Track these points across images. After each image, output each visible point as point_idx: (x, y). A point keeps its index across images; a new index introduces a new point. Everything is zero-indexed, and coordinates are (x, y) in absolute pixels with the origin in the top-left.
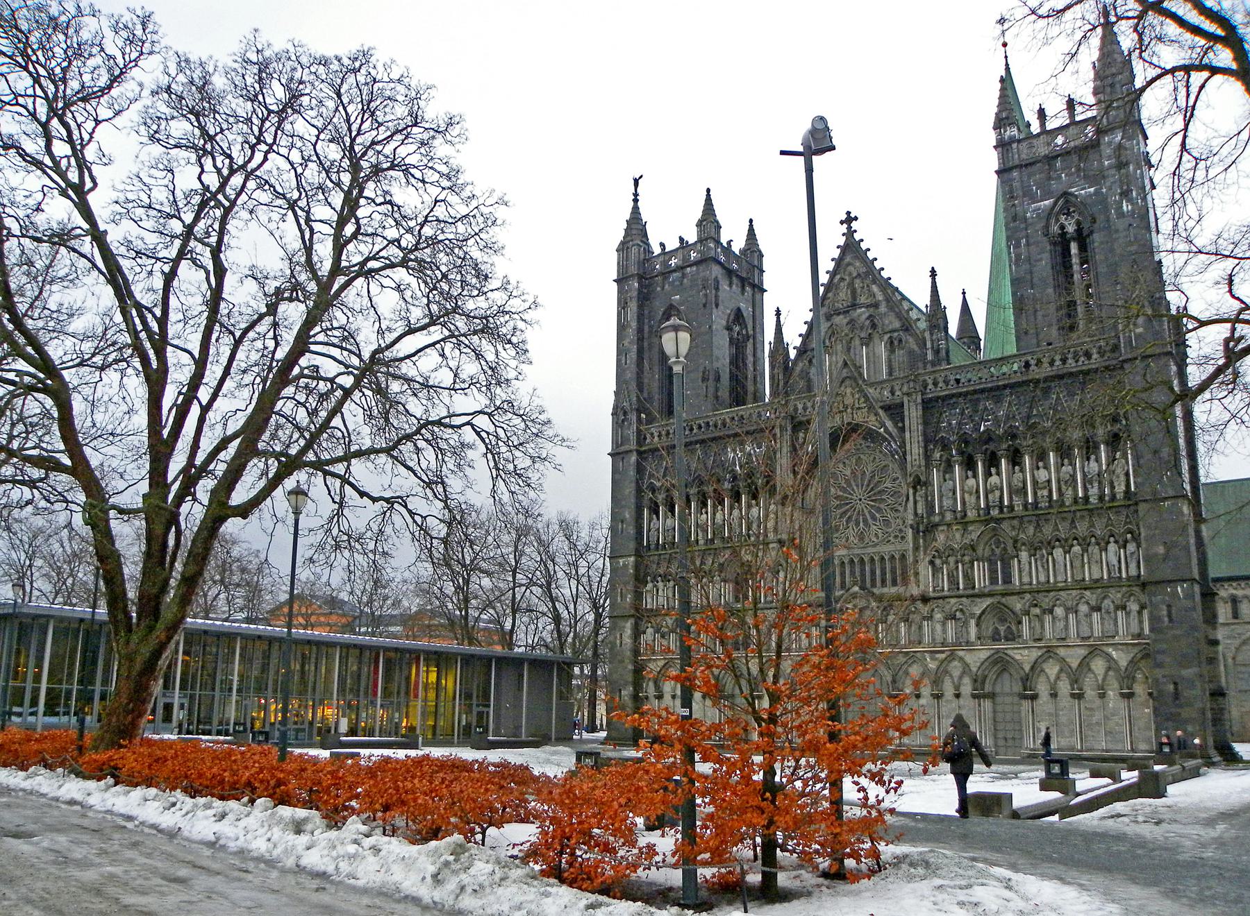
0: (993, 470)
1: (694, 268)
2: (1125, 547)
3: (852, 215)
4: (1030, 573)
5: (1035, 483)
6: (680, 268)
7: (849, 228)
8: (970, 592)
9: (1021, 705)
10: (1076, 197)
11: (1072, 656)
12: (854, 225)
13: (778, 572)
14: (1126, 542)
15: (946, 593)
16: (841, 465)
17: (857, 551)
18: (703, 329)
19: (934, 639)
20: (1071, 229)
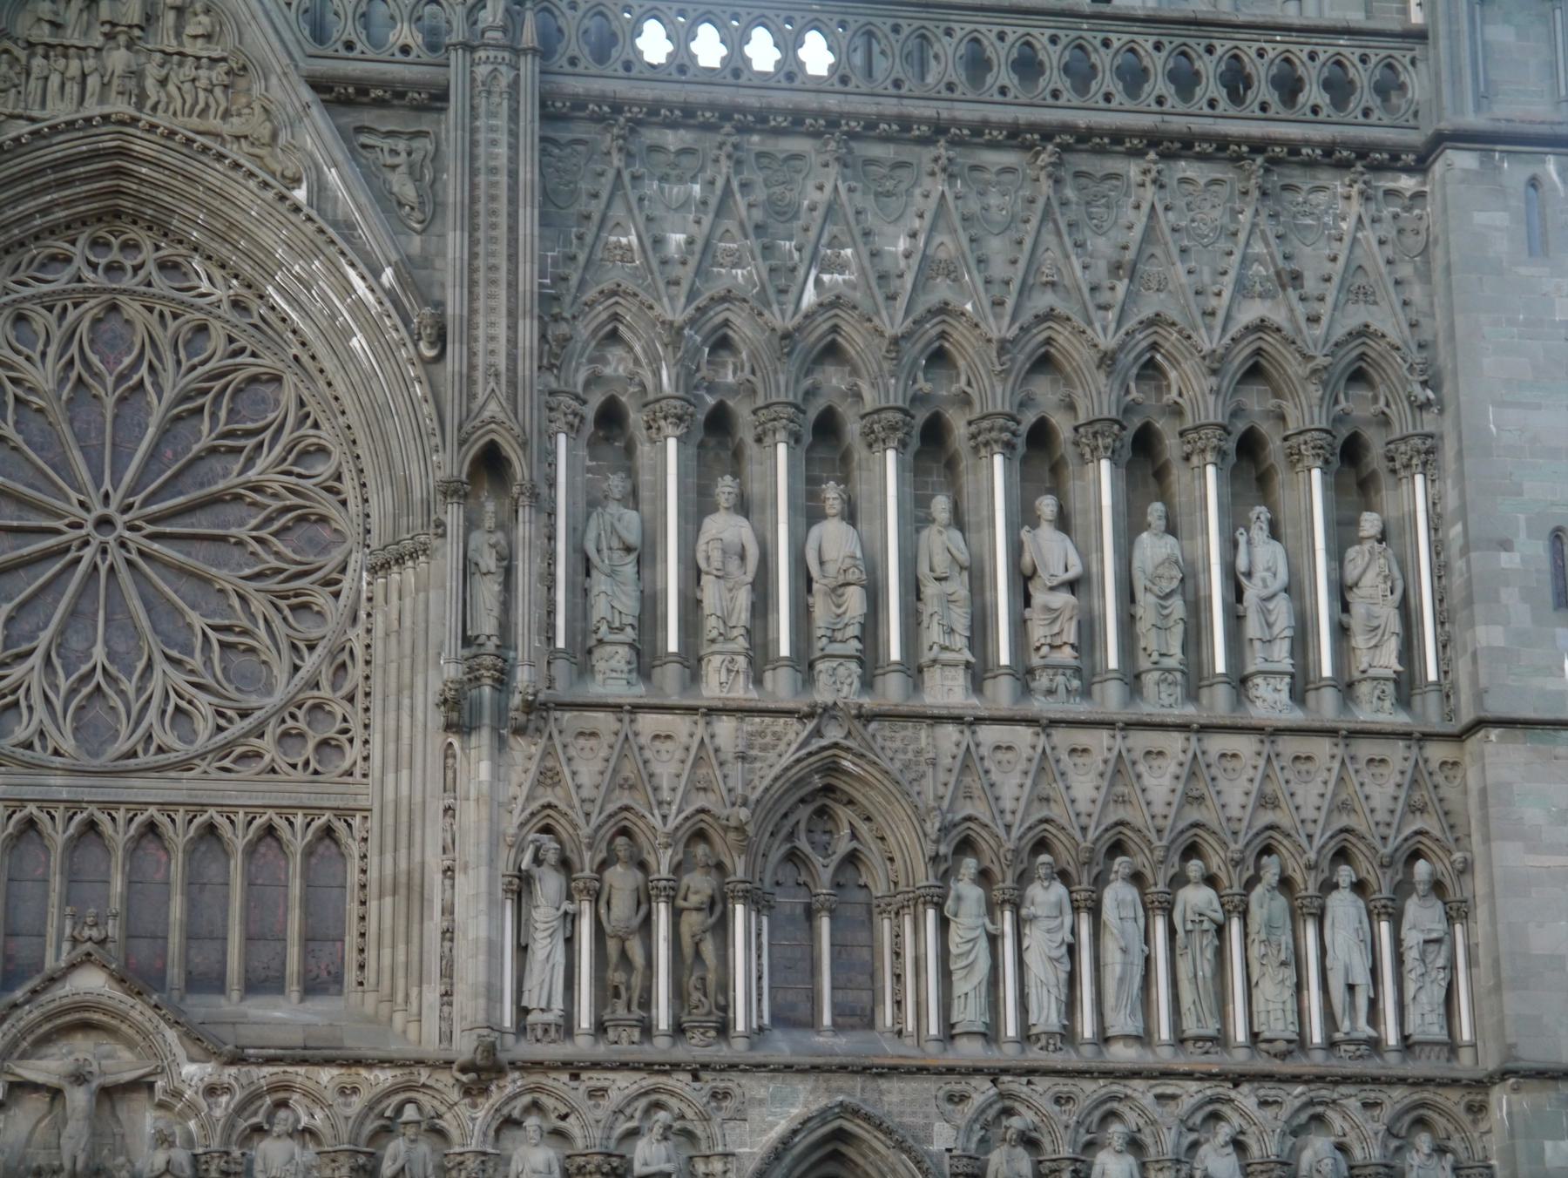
0: (831, 493)
2: (1396, 920)
5: (1023, 581)
8: (695, 1049)
14: (1404, 888)
17: (59, 786)
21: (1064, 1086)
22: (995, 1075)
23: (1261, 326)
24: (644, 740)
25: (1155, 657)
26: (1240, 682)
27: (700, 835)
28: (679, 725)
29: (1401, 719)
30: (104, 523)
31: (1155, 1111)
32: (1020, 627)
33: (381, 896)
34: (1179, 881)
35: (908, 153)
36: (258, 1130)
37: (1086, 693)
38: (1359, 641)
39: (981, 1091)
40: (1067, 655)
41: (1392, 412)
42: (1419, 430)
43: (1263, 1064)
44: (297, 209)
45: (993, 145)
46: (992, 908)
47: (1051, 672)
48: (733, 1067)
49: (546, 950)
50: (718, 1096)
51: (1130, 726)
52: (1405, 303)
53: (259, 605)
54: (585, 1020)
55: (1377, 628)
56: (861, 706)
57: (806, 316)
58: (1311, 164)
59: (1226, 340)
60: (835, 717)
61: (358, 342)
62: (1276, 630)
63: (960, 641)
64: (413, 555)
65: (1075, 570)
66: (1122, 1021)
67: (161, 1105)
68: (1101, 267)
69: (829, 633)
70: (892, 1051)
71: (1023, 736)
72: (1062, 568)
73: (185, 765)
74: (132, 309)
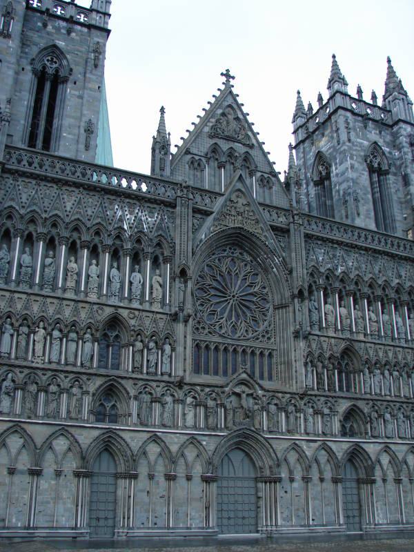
1: (85, 30)
3: (231, 74)
4: (371, 386)
6: (71, 21)
7: (228, 81)
9: (359, 488)
10: (381, 149)
11: (398, 451)
12: (232, 82)
13: (164, 344)
15: (316, 392)
16: (217, 261)
17: (229, 341)
18: (90, 85)
19: (305, 430)
20: (376, 165)
21: (381, 402)
22: (372, 400)
23: (398, 283)
24: (322, 341)
27: (330, 358)
28: (327, 339)
30: (234, 296)
31: (393, 407)
33: (281, 364)
34: (394, 370)
35: (352, 249)
36: (269, 403)
37: (379, 339)
39: (371, 403)
40: (376, 333)
43: (406, 401)
44: (267, 246)
45: (362, 250)
46: (370, 373)
48: (338, 397)
49: (310, 375)
50: (336, 401)
53: (257, 313)
54: (316, 388)
58: (402, 259)
61: (275, 269)
63: (363, 329)
64: (285, 307)
66: (388, 393)
67: (255, 398)
68: (377, 272)
70: (358, 396)
71: (372, 345)
73: (248, 339)
74: (236, 260)
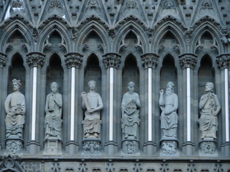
0: (16, 83)
5: (82, 110)
23: (169, 19)
25: (126, 136)
26: (159, 145)
29: (215, 155)
32: (80, 127)
37: (102, 149)
38: (202, 128)
41: (218, 47)
42: (226, 53)
47: (89, 142)
51: (114, 161)
52: (222, 8)
55: (208, 123)
56: (17, 156)
57: (6, 23)
59: (156, 24)
60: (9, 161)
62: (171, 125)
65: (101, 106)
69: (10, 131)
72: (96, 105)
